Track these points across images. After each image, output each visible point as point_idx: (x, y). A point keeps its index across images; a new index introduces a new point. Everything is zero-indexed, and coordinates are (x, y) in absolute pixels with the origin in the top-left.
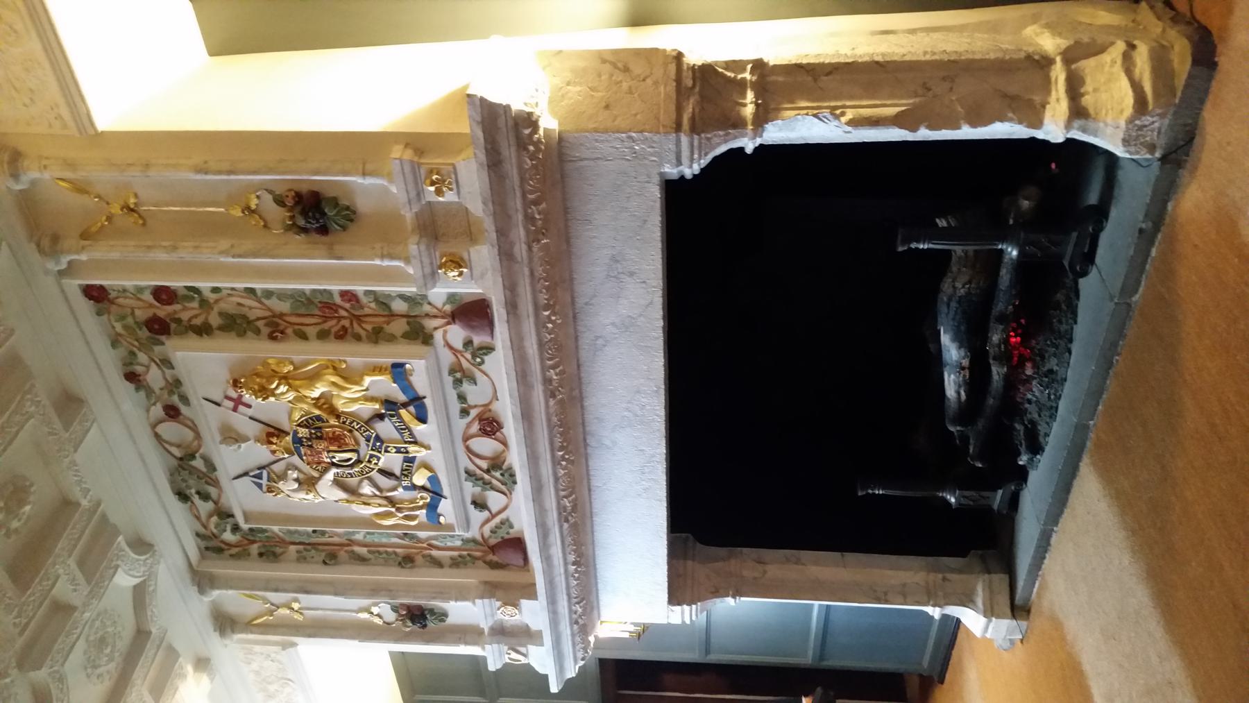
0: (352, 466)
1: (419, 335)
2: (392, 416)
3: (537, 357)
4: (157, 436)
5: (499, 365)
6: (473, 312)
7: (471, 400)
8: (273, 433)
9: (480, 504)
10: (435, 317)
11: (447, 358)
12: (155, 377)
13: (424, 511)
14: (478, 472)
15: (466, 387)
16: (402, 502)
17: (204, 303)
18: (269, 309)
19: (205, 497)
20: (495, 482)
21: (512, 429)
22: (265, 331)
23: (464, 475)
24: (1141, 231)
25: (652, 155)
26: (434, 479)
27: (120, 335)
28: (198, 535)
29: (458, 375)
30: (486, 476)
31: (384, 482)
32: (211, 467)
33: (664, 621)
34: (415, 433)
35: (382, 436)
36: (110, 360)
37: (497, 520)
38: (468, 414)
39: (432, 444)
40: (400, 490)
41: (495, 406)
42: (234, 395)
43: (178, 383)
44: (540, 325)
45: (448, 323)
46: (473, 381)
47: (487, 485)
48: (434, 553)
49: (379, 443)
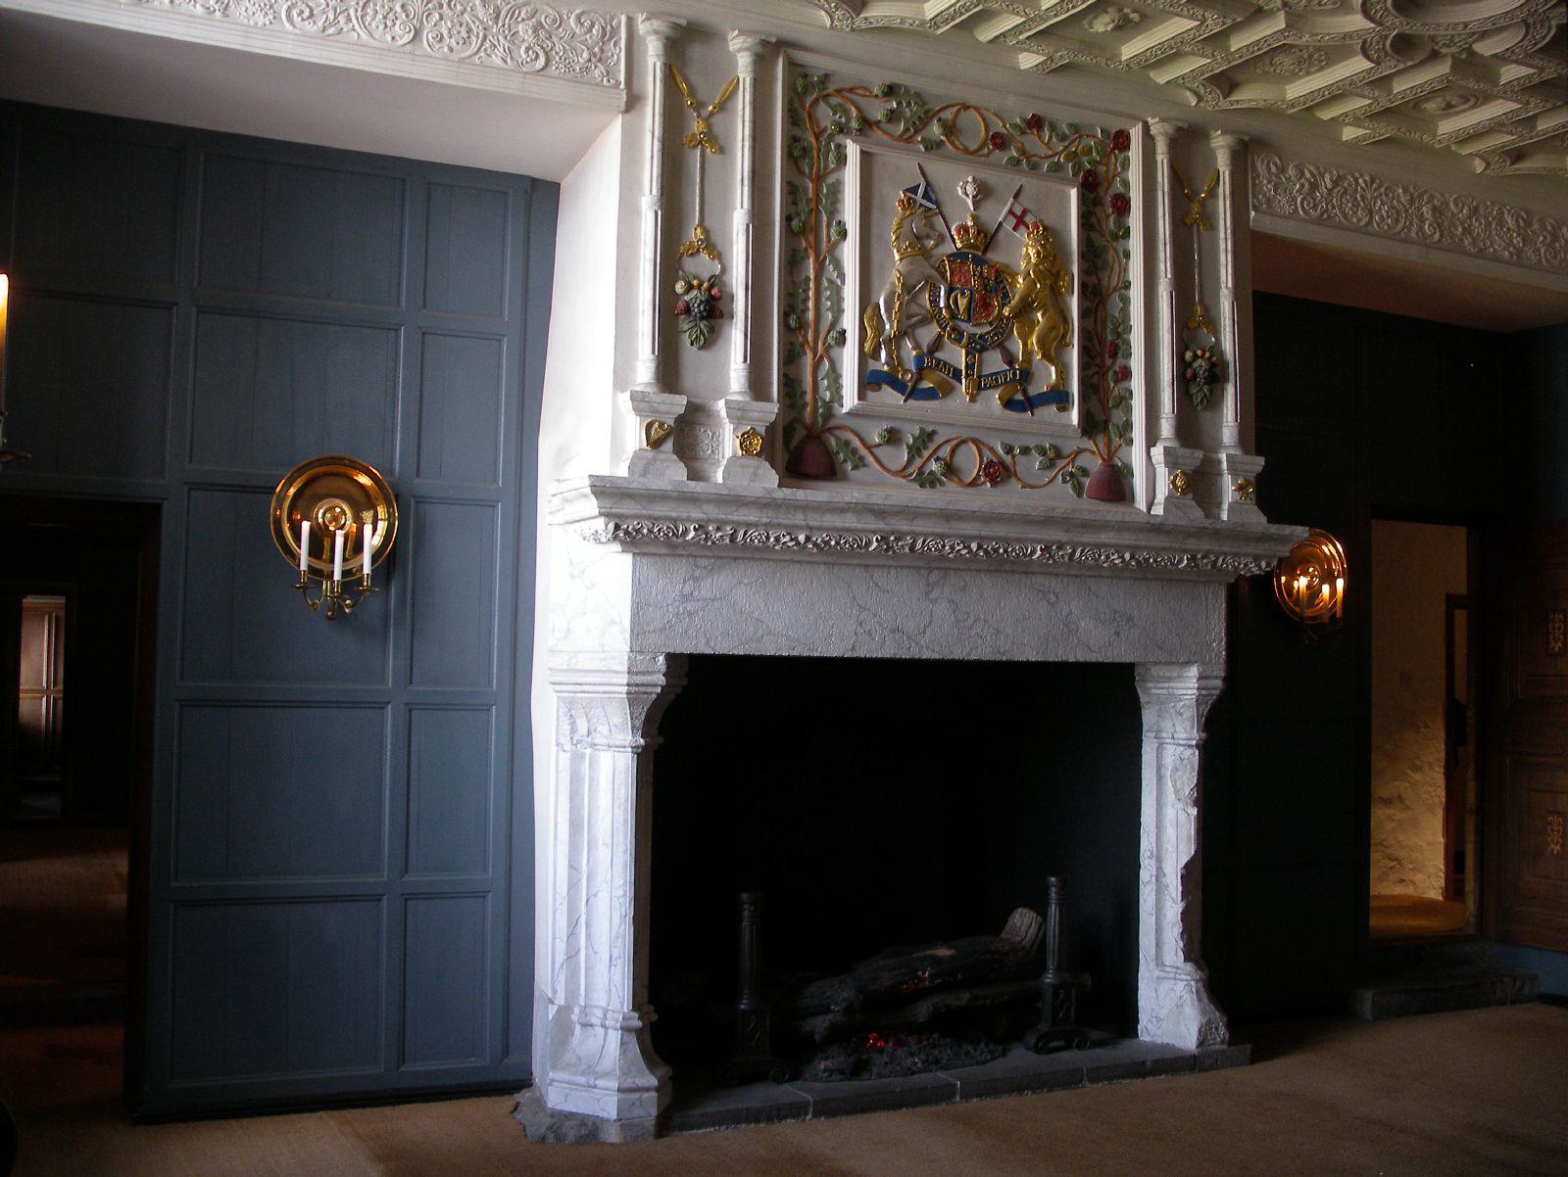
0: (948, 306)
1: (1091, 425)
2: (1014, 374)
3: (1097, 541)
4: (967, 107)
5: (1059, 496)
6: (1116, 485)
7: (1021, 460)
8: (986, 238)
9: (892, 437)
10: (1109, 448)
11: (1069, 447)
12: (1034, 143)
13: (886, 368)
14: (932, 447)
15: (1037, 461)
16: (898, 348)
17: (1116, 237)
18: (1109, 296)
19: (893, 116)
20: (918, 462)
21: (987, 498)
22: (1093, 280)
23: (930, 429)
24: (1144, 1063)
25: (1210, 656)
26: (930, 395)
27: (1081, 137)
28: (827, 76)
29: (1051, 454)
30: (926, 454)
31: (928, 334)
32: (932, 146)
33: (1040, 658)
34: (991, 391)
35: (986, 355)
36: (1064, 117)
37: (863, 451)
38: (1007, 453)
39: (977, 406)
40: (914, 353)
41: (1014, 485)
42: (1029, 219)
43: (1034, 167)
44: (1119, 549)
45: (1104, 459)
46: (1045, 468)
47: (915, 451)
48: (808, 359)
49: (977, 347)
